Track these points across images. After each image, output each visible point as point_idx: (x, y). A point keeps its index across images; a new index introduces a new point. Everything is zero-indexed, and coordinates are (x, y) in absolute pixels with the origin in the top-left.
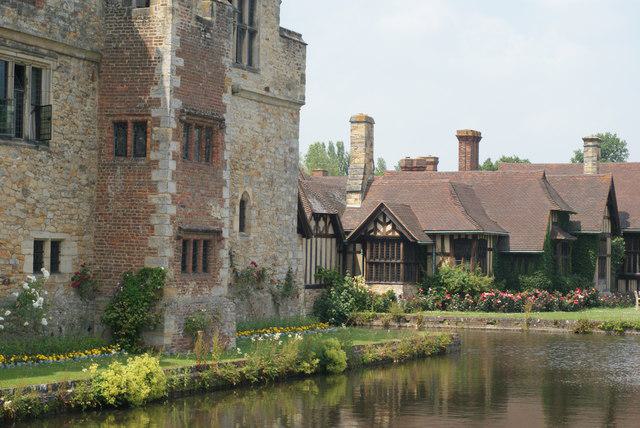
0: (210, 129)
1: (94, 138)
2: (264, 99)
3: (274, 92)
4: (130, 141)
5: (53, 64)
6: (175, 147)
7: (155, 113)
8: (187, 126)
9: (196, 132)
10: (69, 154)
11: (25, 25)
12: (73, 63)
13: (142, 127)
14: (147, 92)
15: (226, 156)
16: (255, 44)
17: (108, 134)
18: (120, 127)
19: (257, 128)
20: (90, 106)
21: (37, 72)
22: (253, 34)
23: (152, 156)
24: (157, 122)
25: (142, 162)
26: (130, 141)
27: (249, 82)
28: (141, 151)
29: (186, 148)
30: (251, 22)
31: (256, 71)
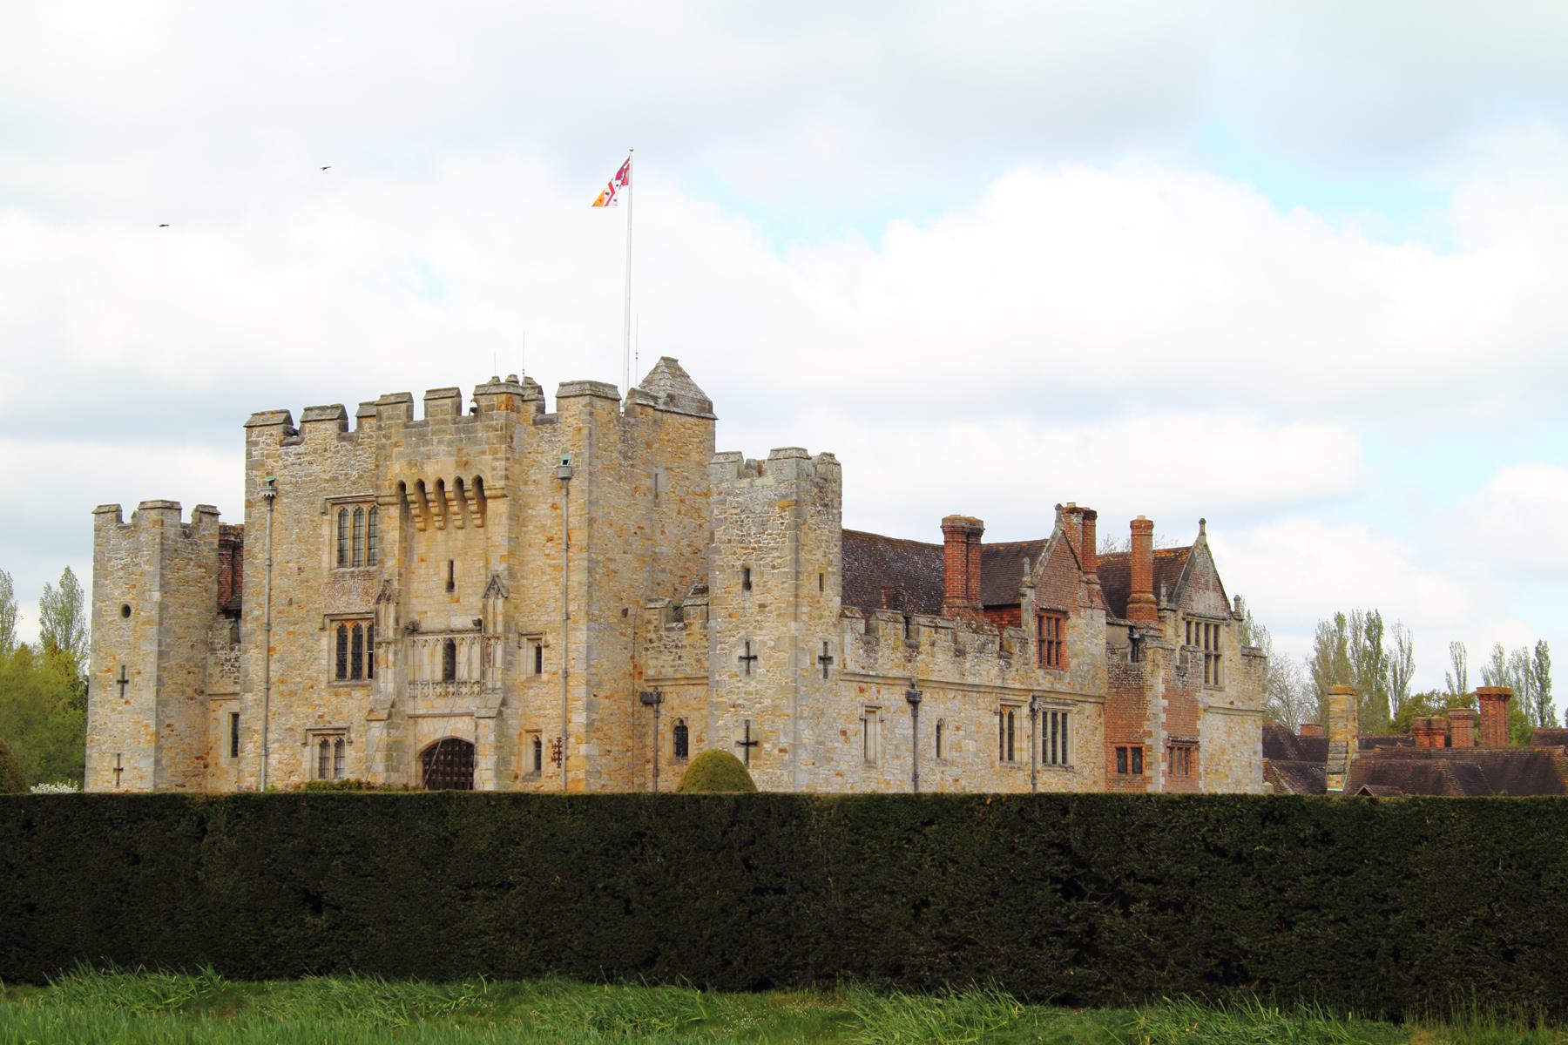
0: (1188, 749)
1: (1102, 759)
2: (1228, 711)
3: (1238, 705)
4: (1130, 762)
5: (1075, 709)
6: (1164, 766)
7: (1148, 741)
8: (1171, 749)
9: (1176, 753)
10: (1086, 773)
11: (1058, 687)
12: (1087, 706)
13: (1138, 751)
14: (1141, 726)
15: (1201, 769)
16: (1220, 666)
17: (1113, 756)
18: (1121, 751)
19: (1224, 736)
20: (1100, 736)
21: (1064, 716)
22: (1217, 657)
23: (1147, 773)
24: (1150, 748)
25: (1139, 777)
26: (1130, 762)
27: (1217, 700)
28: (1138, 769)
29: (1171, 766)
30: (1216, 648)
31: (1221, 690)
